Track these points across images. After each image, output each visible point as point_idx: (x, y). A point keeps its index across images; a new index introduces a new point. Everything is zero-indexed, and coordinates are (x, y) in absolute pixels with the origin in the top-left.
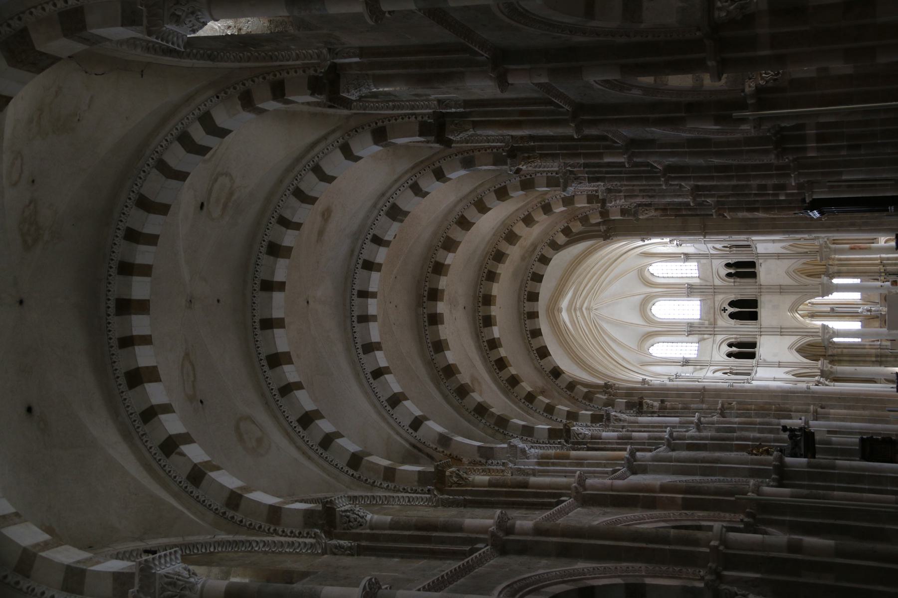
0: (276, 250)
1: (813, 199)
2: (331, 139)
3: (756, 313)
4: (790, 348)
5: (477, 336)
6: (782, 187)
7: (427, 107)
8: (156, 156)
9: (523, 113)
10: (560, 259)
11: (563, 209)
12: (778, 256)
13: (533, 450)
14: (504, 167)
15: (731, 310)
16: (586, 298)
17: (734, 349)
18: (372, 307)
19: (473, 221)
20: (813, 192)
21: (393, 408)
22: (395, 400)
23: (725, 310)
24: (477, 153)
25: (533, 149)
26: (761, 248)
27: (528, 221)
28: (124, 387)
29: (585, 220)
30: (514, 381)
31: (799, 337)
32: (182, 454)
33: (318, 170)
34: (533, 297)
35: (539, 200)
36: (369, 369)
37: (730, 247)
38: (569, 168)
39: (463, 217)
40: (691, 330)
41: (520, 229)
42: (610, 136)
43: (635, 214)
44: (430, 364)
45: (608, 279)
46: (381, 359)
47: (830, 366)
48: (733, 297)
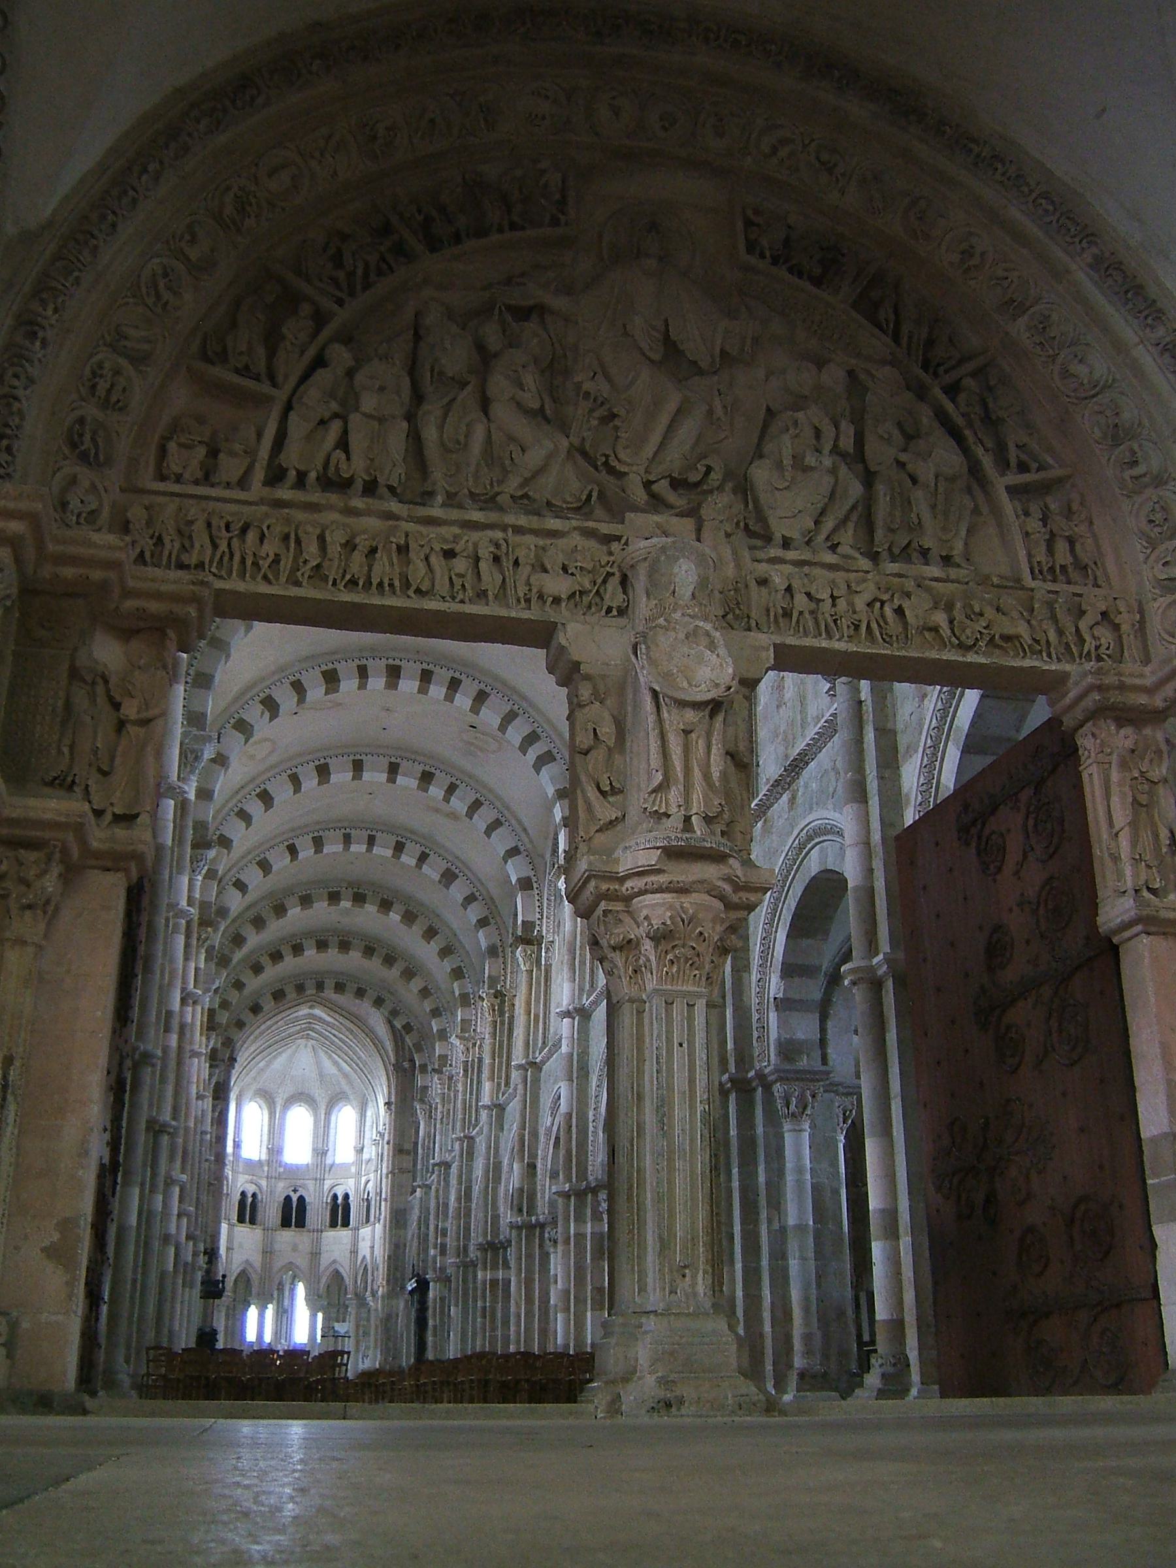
0: (426, 778)
1: (429, 1283)
2: (526, 840)
3: (290, 1226)
4: (247, 1261)
5: (309, 934)
6: (443, 1252)
7: (548, 931)
8: (521, 711)
9: (537, 1016)
10: (377, 1020)
11: (435, 1030)
12: (354, 1252)
13: (208, 999)
14: (486, 986)
15: (295, 1198)
16: (320, 1034)
17: (250, 1200)
18: (358, 848)
19: (432, 942)
20: (436, 1282)
21: (257, 863)
22: (265, 866)
23: (295, 1191)
24: (501, 960)
25: (502, 1013)
26: (365, 1232)
27: (425, 993)
28: (324, 668)
29: (418, 1048)
30: (257, 969)
31: (259, 1270)
32: (263, 713)
33: (495, 825)
34: (340, 988)
35: (446, 1005)
36: (297, 842)
37: (367, 1199)
38: (478, 1043)
39: (436, 933)
40: (275, 1150)
41: (416, 985)
42: (511, 1091)
43: (422, 1101)
44: (289, 892)
45: (340, 1061)
46: (306, 852)
47: (226, 1304)
48: (307, 1200)
